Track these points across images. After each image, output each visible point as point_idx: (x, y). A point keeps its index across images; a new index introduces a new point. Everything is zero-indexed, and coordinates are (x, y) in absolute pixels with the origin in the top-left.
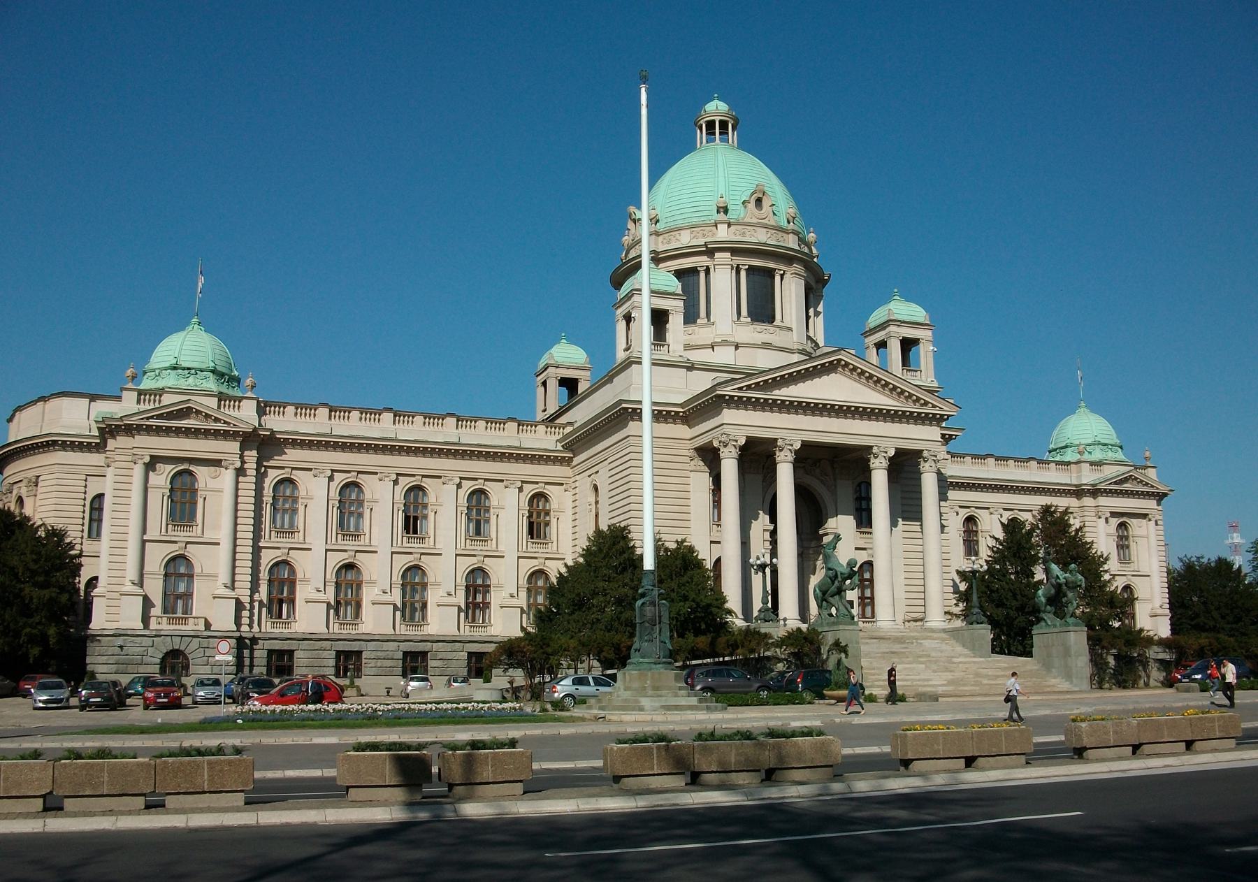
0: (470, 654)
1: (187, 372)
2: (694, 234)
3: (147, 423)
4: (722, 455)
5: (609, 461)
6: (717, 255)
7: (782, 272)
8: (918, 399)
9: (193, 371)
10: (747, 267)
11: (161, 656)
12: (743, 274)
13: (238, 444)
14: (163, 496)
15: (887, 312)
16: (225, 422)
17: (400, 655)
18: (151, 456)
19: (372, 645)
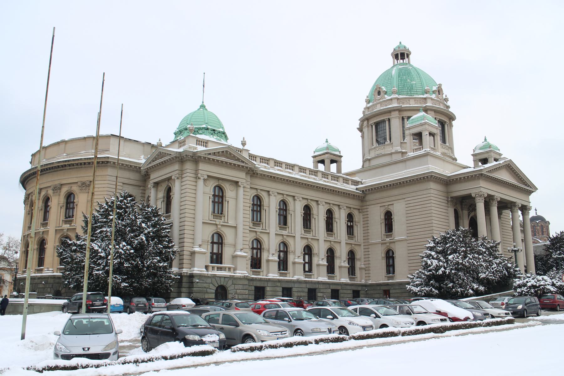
0: (332, 290)
1: (212, 132)
2: (416, 101)
3: (209, 157)
4: (476, 201)
5: (406, 200)
8: (527, 184)
9: (216, 132)
10: (438, 119)
11: (215, 288)
13: (244, 174)
14: (210, 198)
16: (243, 162)
17: (306, 290)
18: (208, 176)
19: (296, 285)
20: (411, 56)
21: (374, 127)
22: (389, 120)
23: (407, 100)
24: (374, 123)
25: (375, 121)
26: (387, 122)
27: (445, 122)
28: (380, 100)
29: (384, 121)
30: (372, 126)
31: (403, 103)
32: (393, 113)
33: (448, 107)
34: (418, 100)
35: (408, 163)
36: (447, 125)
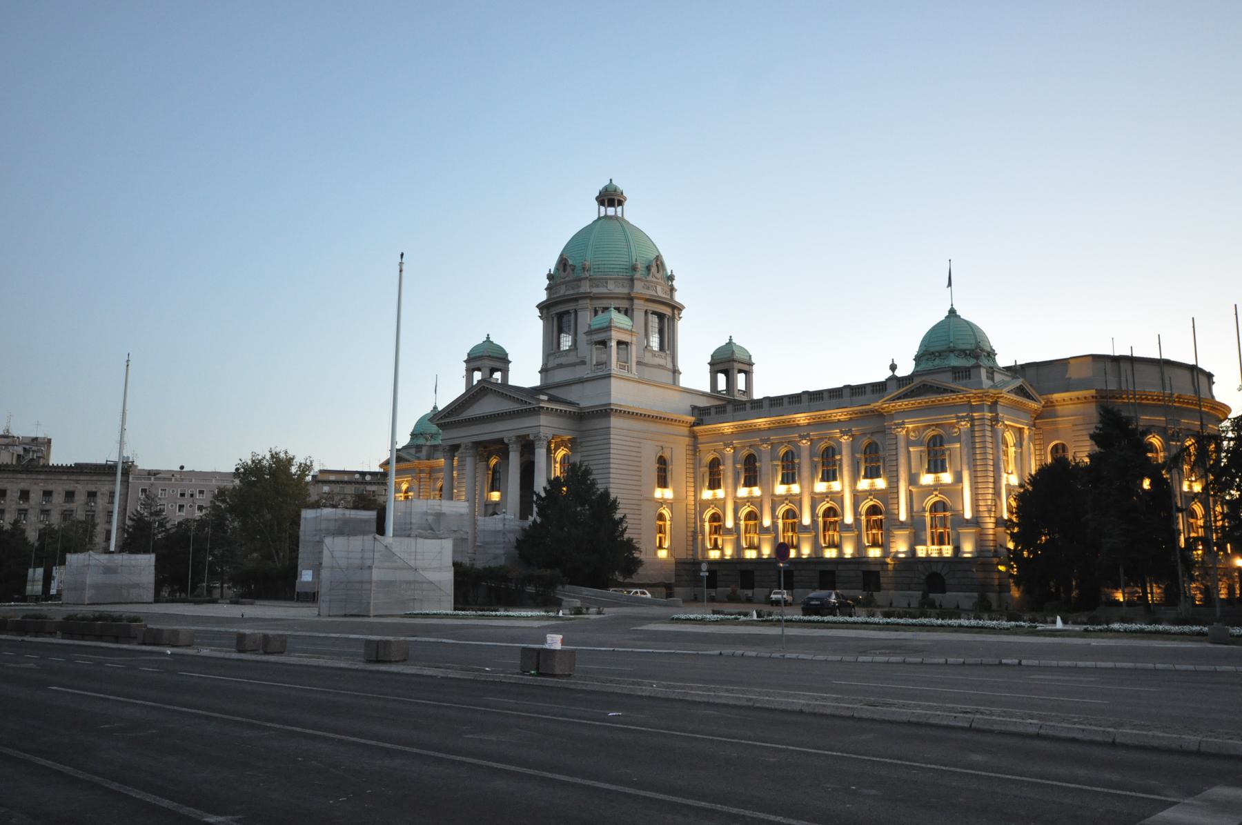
6: (636, 302)
7: (667, 317)
12: (650, 315)
15: (730, 352)
20: (626, 204)
21: (555, 319)
22: (576, 312)
23: (604, 281)
24: (557, 314)
25: (557, 311)
26: (573, 315)
27: (665, 315)
28: (565, 278)
29: (568, 312)
30: (553, 318)
31: (598, 286)
32: (580, 302)
33: (672, 289)
34: (620, 281)
35: (585, 384)
36: (668, 319)
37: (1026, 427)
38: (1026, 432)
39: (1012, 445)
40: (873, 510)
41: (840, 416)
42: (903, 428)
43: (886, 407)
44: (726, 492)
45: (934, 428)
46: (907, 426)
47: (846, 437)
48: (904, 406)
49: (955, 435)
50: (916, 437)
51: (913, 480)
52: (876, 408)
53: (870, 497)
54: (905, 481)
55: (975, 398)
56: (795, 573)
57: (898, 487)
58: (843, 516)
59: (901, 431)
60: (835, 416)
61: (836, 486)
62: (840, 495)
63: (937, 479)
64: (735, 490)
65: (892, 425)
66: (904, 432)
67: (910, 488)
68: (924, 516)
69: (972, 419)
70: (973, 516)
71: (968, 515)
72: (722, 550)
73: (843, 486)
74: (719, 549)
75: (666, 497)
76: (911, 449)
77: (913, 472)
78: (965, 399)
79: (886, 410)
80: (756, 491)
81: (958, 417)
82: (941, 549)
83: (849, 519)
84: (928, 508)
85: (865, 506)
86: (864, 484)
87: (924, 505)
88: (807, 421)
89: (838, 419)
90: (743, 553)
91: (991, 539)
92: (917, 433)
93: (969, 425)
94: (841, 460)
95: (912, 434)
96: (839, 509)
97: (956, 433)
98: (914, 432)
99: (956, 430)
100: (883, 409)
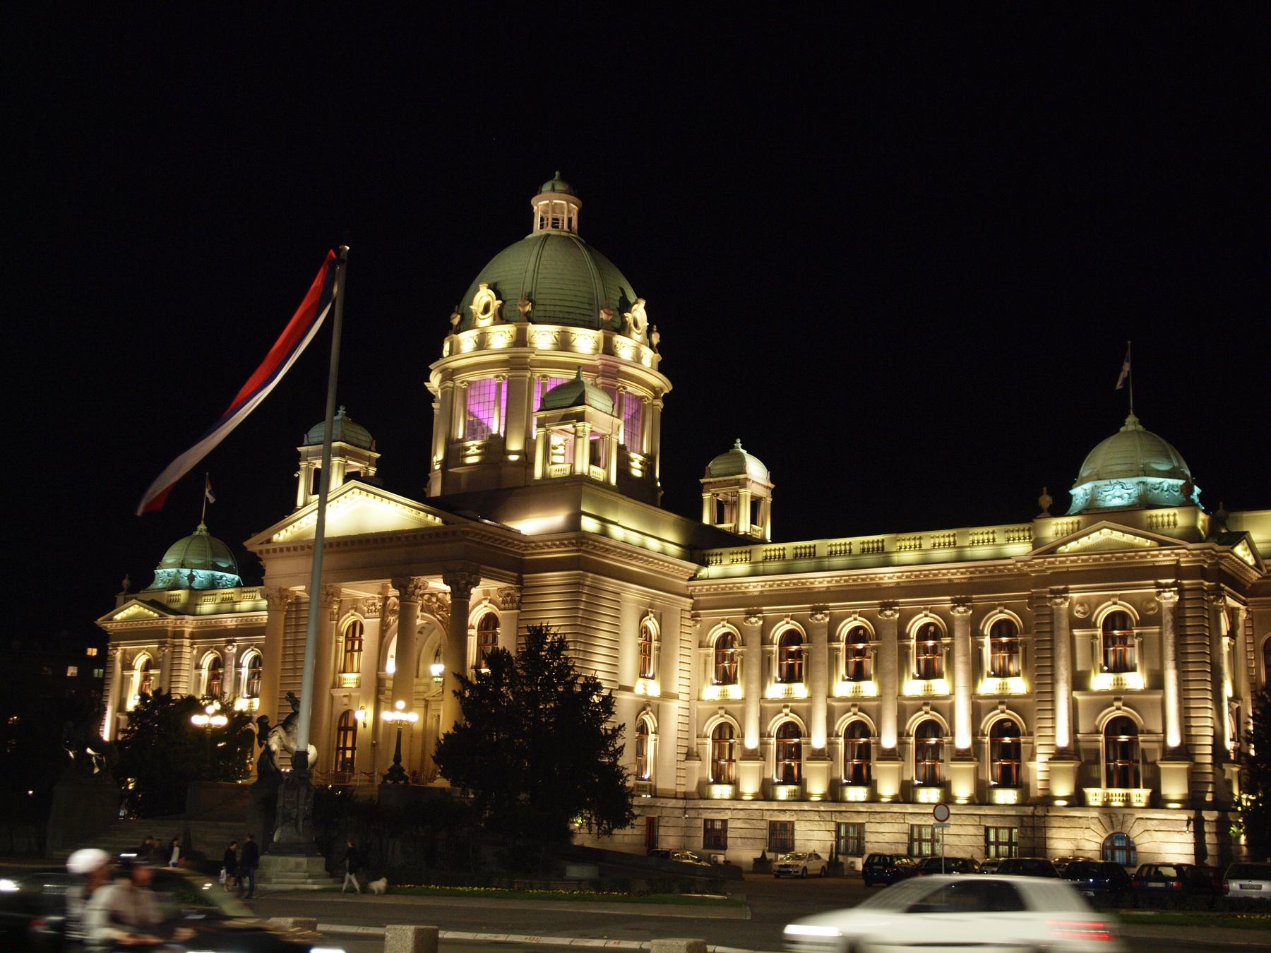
37: (1242, 607)
38: (1243, 615)
39: (1226, 634)
40: (1001, 729)
41: (953, 574)
42: (1066, 599)
43: (1036, 564)
44: (747, 690)
45: (1116, 600)
46: (1070, 595)
47: (961, 609)
48: (1068, 563)
49: (1151, 613)
50: (1084, 613)
51: (1079, 682)
52: (1019, 565)
53: (1001, 707)
54: (1067, 682)
55: (1187, 556)
56: (868, 827)
57: (1053, 693)
58: (953, 734)
59: (1061, 603)
60: (944, 575)
61: (940, 687)
62: (949, 701)
63: (1119, 682)
64: (763, 687)
65: (1046, 592)
66: (1067, 604)
67: (1075, 694)
68: (1099, 741)
69: (1181, 592)
70: (1182, 743)
71: (1174, 740)
72: (734, 783)
73: (954, 686)
74: (730, 783)
75: (650, 693)
76: (1077, 632)
77: (1079, 668)
78: (1173, 557)
79: (1037, 568)
80: (800, 690)
81: (1158, 586)
82: (1128, 795)
83: (963, 740)
84: (1102, 727)
85: (988, 722)
86: (989, 686)
87: (1097, 723)
88: (895, 580)
89: (950, 580)
90: (843, 792)
91: (1211, 780)
92: (1086, 606)
93: (1177, 598)
94: (951, 645)
95: (1078, 608)
96: (945, 725)
97: (1153, 609)
98: (1082, 605)
99: (1153, 605)
100: (1030, 566)
